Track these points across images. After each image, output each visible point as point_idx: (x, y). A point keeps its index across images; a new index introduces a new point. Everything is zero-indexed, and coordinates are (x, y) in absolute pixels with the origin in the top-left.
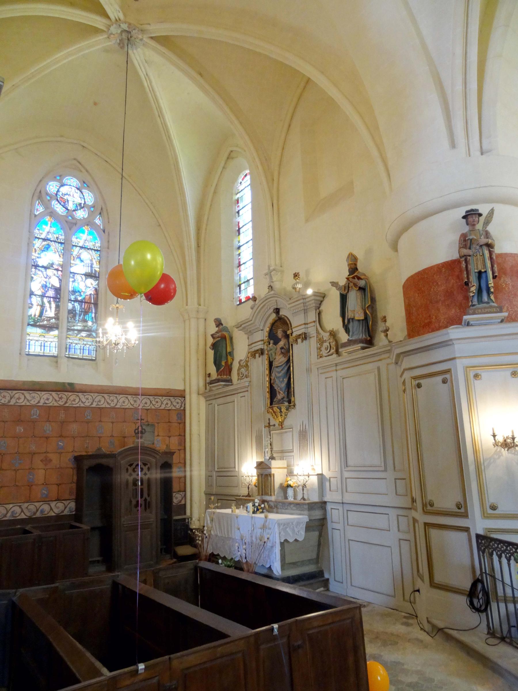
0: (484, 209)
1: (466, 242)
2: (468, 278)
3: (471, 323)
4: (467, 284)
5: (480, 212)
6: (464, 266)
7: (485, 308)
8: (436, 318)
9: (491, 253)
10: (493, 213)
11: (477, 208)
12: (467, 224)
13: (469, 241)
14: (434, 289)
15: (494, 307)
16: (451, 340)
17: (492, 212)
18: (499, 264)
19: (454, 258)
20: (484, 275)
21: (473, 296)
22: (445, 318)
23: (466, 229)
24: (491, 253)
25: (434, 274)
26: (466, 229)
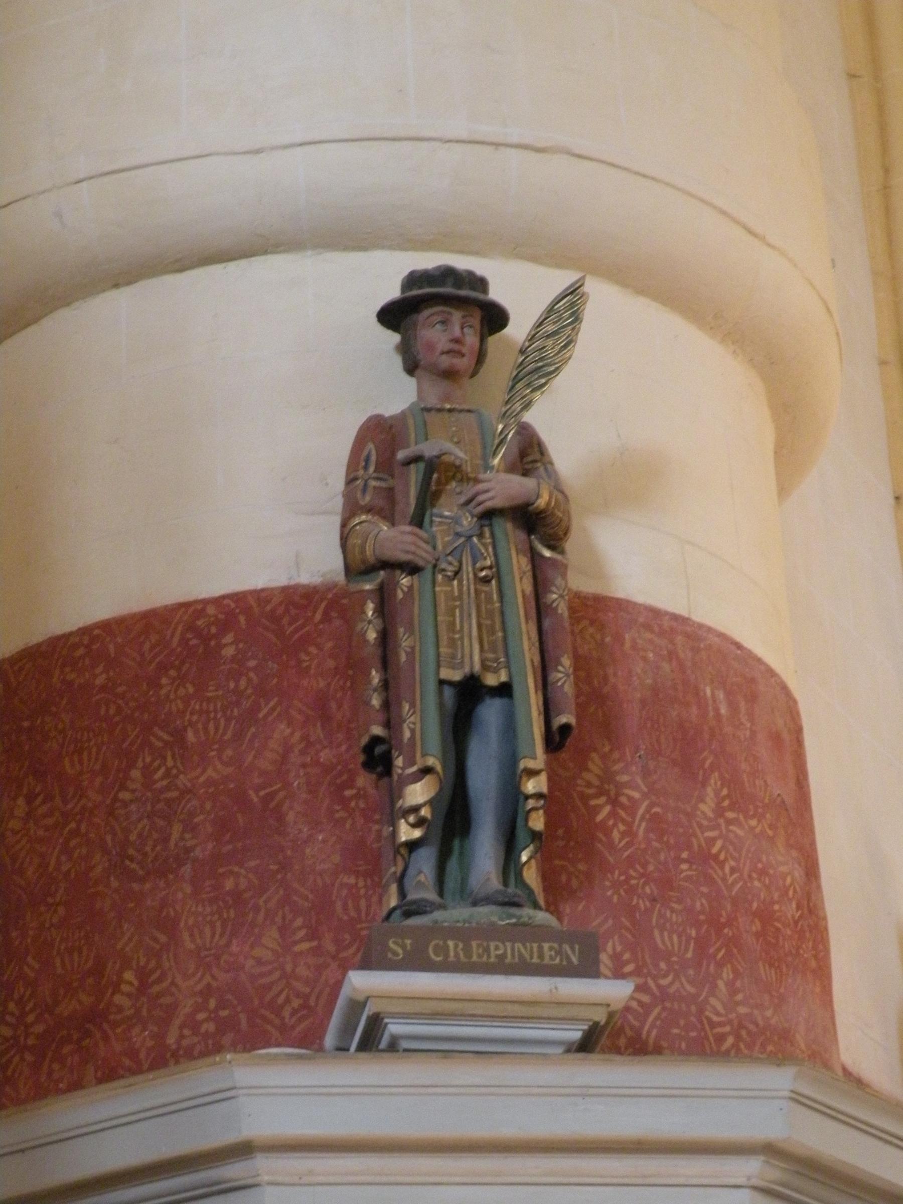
0: (522, 291)
1: (391, 470)
2: (390, 714)
3: (394, 1028)
4: (378, 758)
5: (496, 294)
6: (372, 636)
7: (490, 932)
8: (144, 986)
9: (540, 586)
10: (577, 318)
11: (479, 272)
12: (411, 367)
13: (415, 474)
14: (148, 773)
15: (539, 933)
16: (244, 1150)
17: (566, 311)
18: (579, 662)
19: (306, 578)
20: (490, 712)
21: (413, 846)
22: (207, 993)
23: (397, 394)
24: (540, 586)
25: (163, 668)
26: (397, 394)
